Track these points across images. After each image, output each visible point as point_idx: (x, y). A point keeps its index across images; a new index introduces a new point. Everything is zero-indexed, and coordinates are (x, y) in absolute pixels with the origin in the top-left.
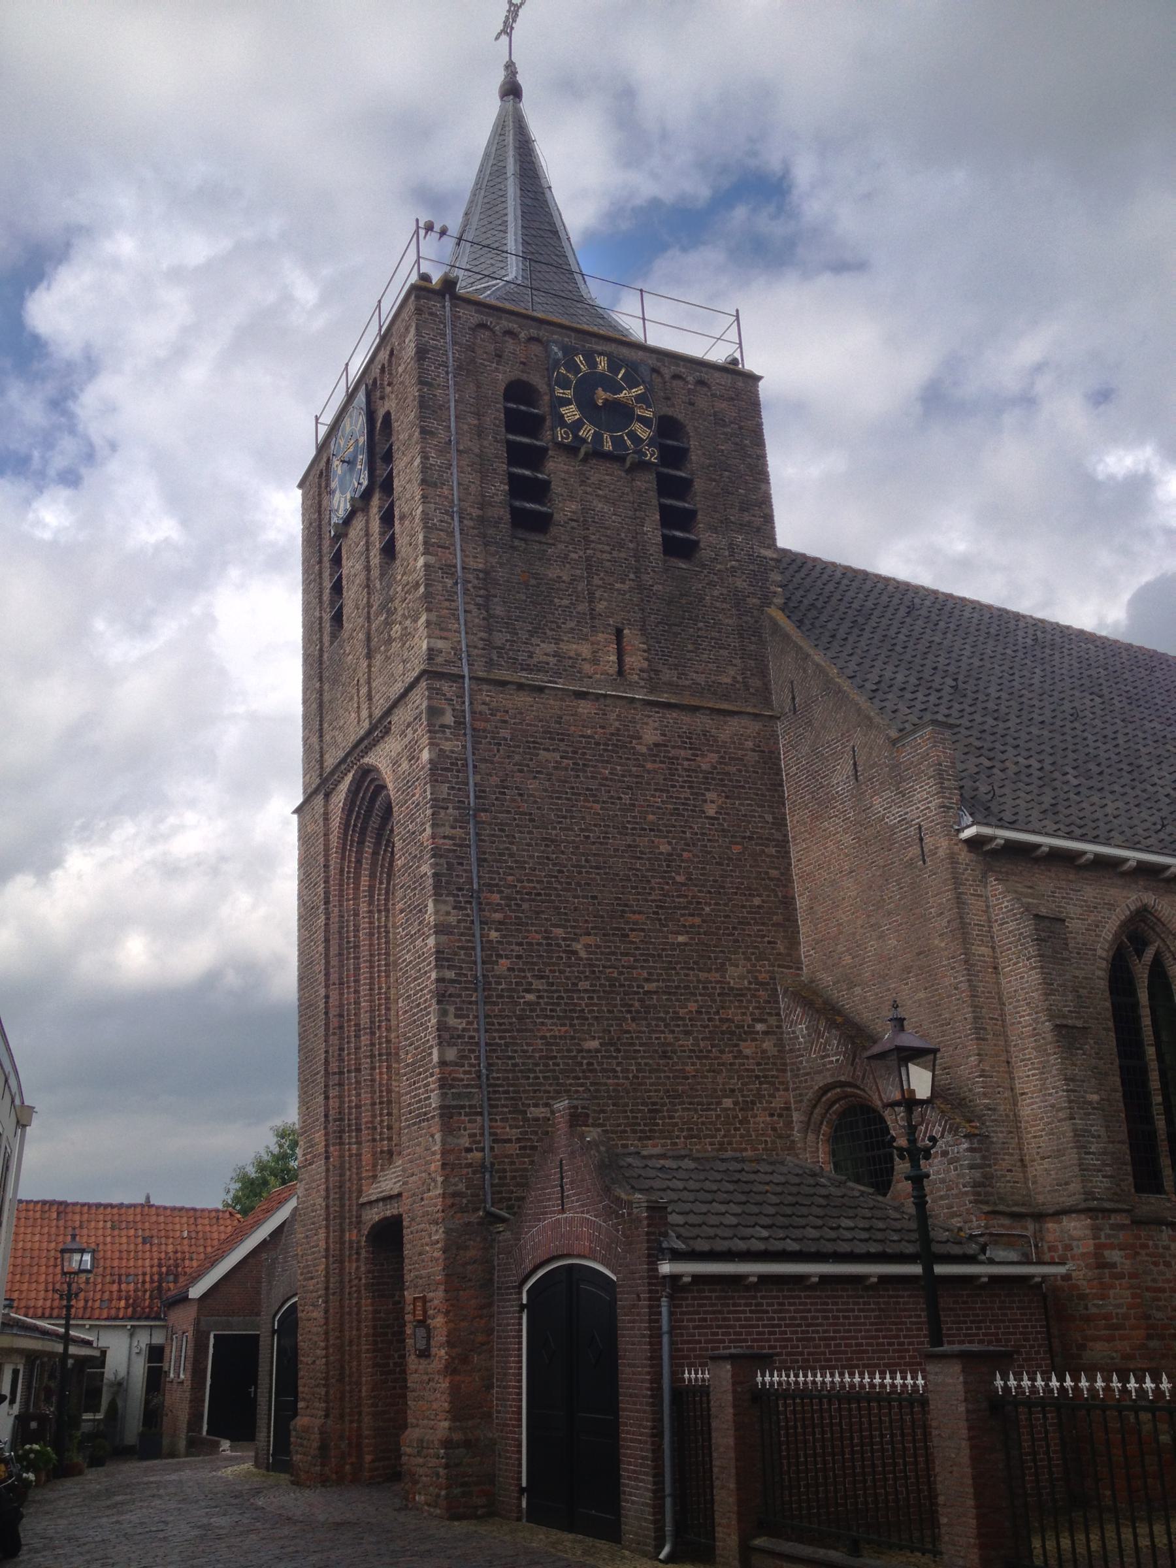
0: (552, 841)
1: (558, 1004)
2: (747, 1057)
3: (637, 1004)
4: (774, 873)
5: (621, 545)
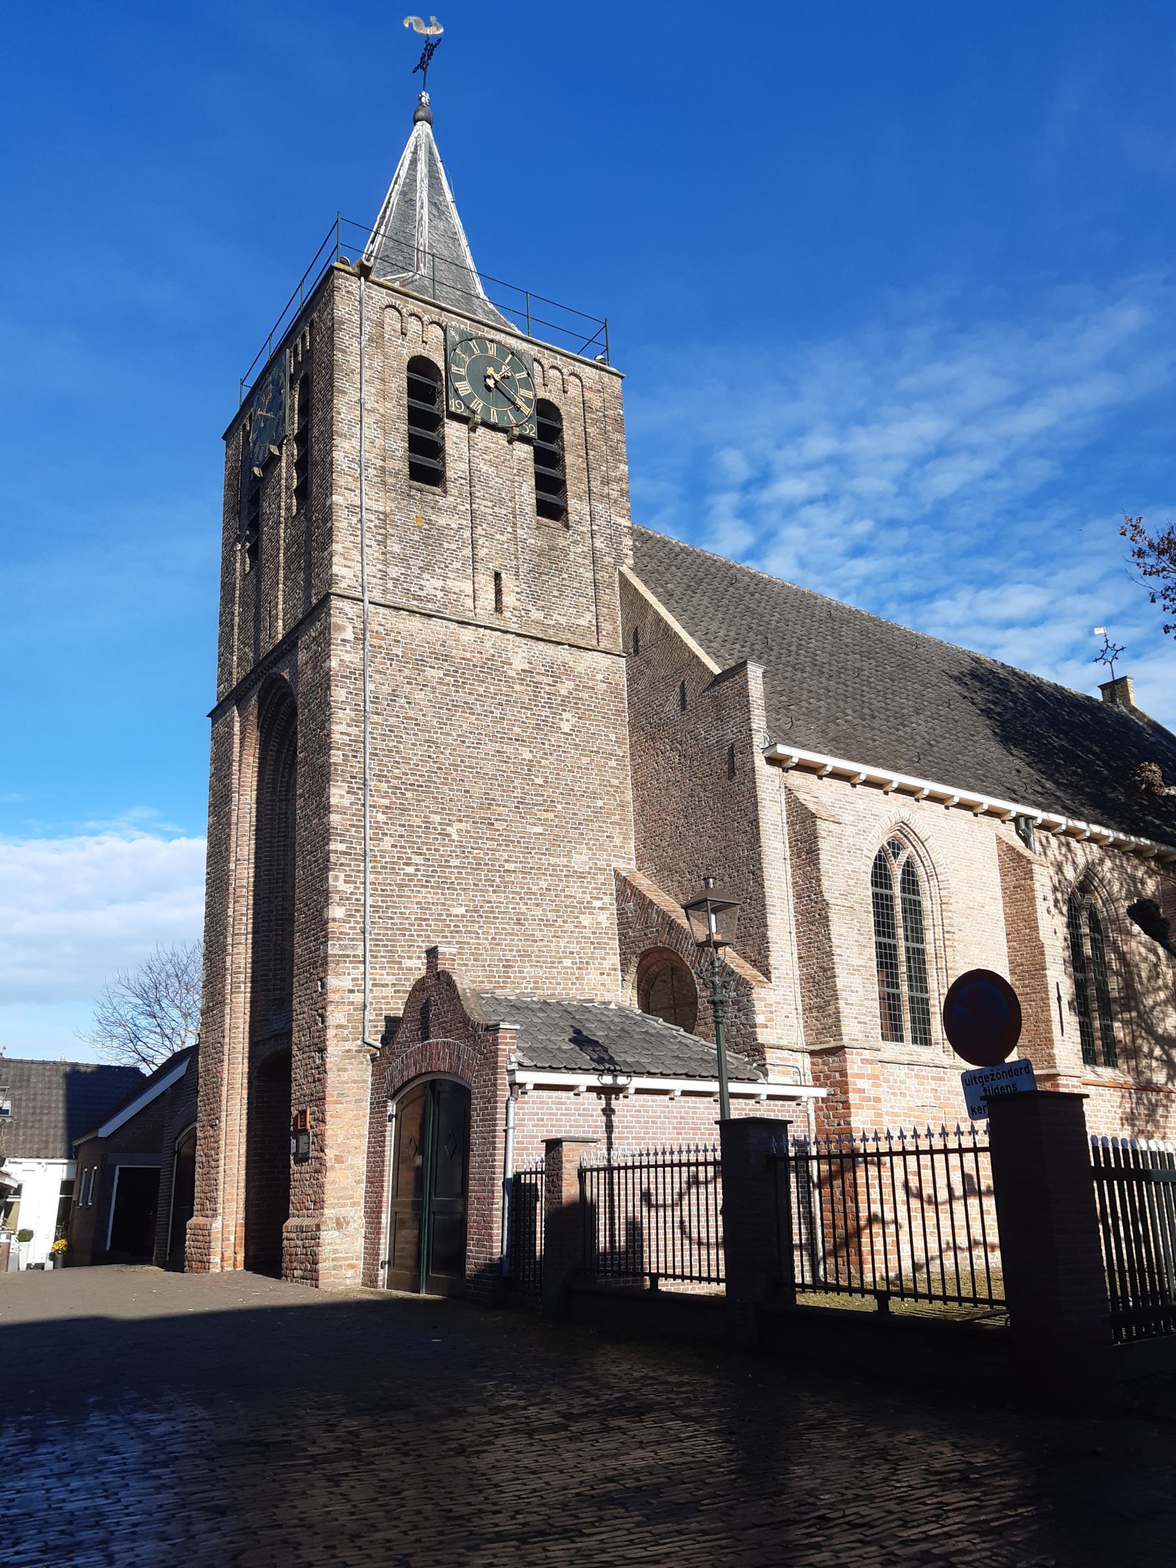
1: (433, 877)
3: (498, 880)
5: (501, 502)
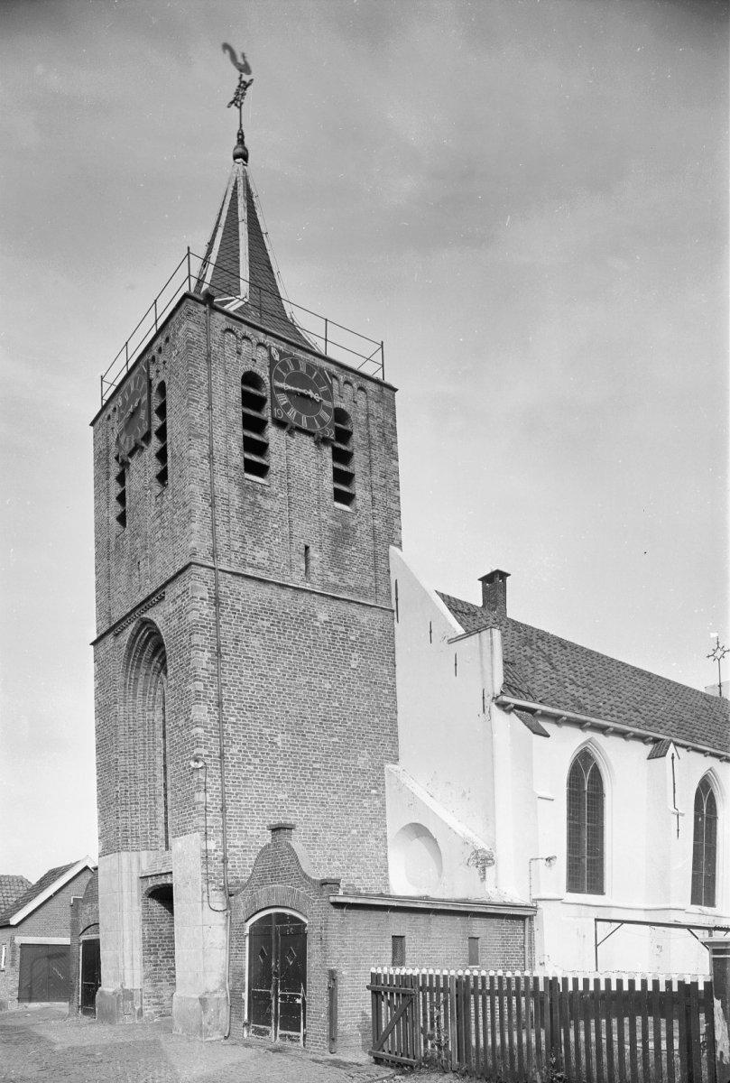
0: (264, 676)
4: (387, 705)
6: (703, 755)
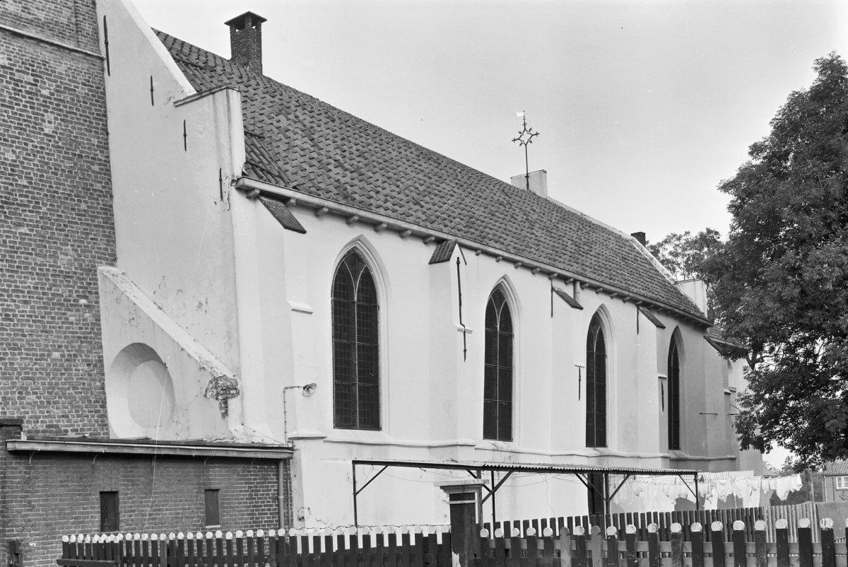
2: (72, 323)
4: (99, 186)
6: (494, 260)
